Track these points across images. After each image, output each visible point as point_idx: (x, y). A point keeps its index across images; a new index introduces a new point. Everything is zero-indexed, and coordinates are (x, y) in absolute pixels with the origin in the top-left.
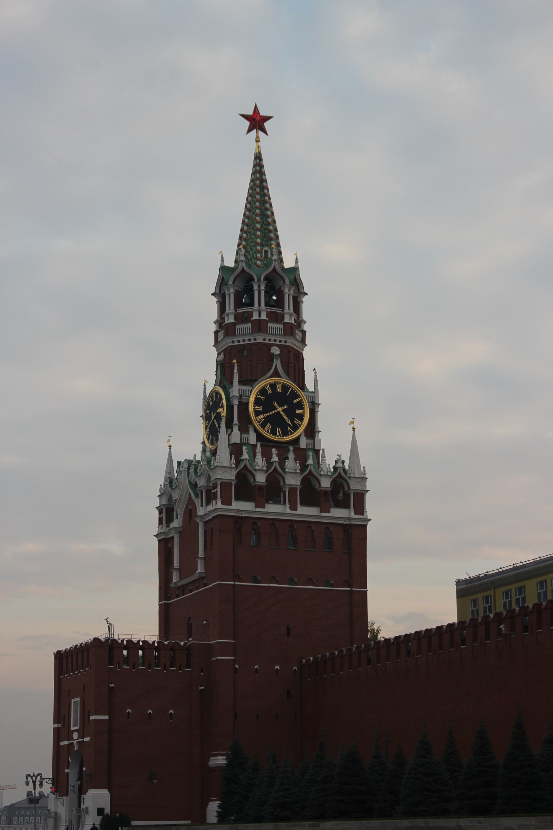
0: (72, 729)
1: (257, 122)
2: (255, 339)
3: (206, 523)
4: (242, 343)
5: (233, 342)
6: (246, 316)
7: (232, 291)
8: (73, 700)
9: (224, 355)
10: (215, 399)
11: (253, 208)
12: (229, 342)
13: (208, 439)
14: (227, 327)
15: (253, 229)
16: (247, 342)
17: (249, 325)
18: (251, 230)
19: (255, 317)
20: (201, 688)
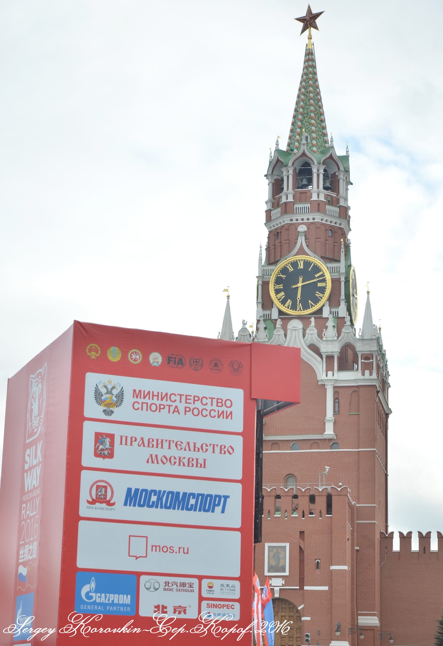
0: (267, 574)
1: (309, 21)
2: (340, 225)
3: (335, 387)
4: (329, 223)
5: (322, 220)
6: (329, 199)
7: (322, 171)
8: (267, 545)
9: (308, 228)
10: (301, 266)
11: (315, 99)
12: (318, 217)
13: (283, 302)
14: (319, 204)
15: (318, 119)
16: (333, 224)
17: (337, 209)
18: (316, 119)
19: (342, 203)
20: (358, 548)
